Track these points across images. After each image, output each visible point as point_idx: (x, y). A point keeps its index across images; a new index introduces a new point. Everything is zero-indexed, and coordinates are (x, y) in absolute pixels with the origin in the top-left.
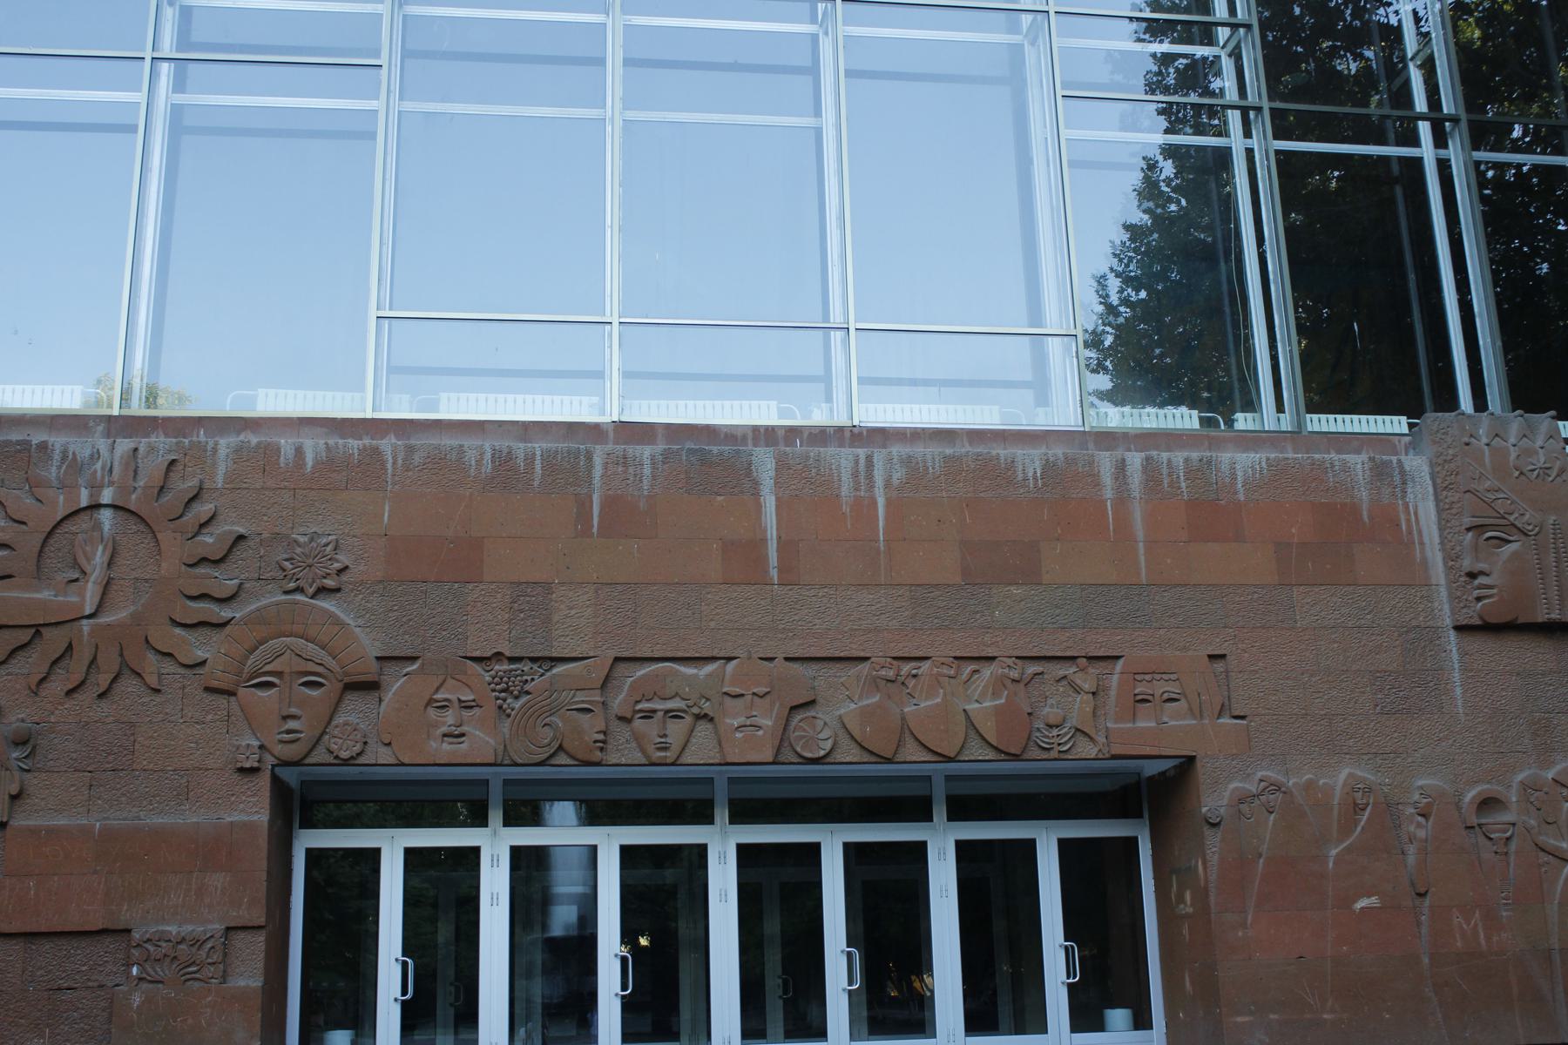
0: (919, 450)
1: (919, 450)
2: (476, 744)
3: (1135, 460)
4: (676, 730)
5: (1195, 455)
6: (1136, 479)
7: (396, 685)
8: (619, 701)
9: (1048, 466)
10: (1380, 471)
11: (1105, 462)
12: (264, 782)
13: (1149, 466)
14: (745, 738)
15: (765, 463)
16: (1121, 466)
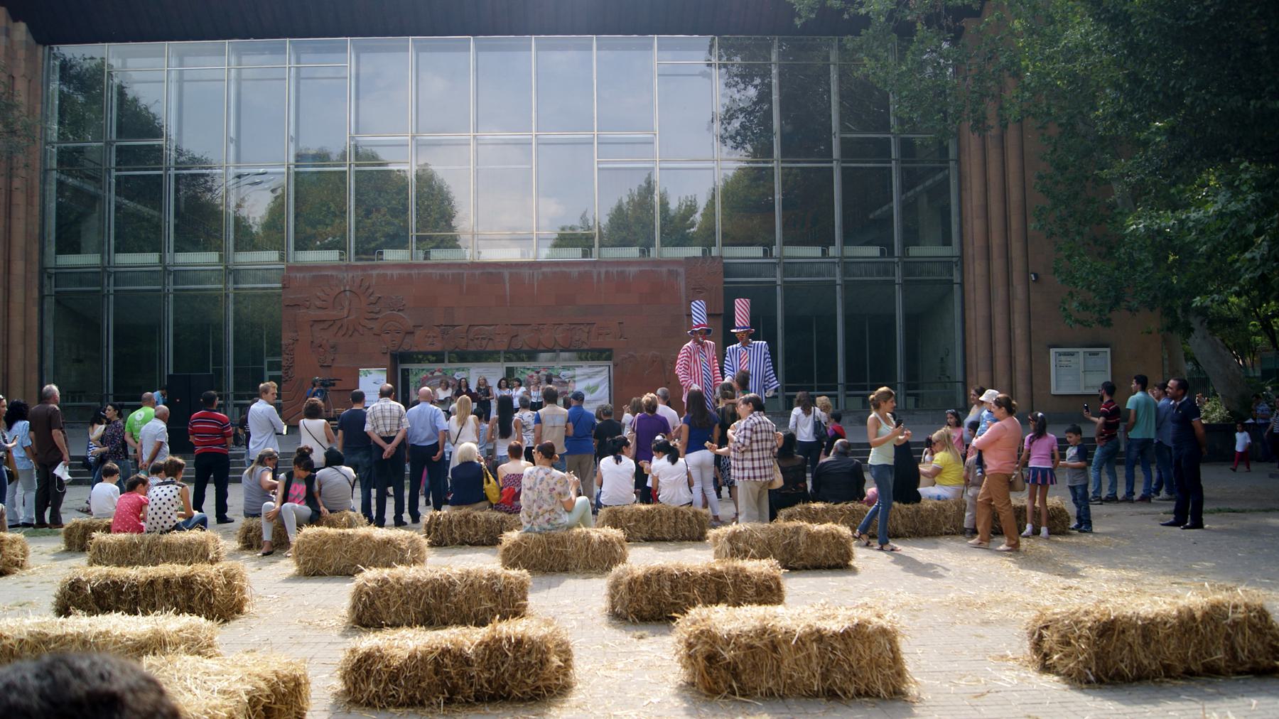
0: (544, 269)
1: (544, 269)
2: (437, 347)
3: (603, 270)
4: (484, 343)
5: (620, 269)
6: (603, 276)
7: (418, 332)
8: (471, 336)
9: (580, 273)
10: (670, 272)
11: (595, 271)
12: (388, 356)
13: (607, 272)
14: (501, 344)
15: (506, 273)
16: (599, 274)
